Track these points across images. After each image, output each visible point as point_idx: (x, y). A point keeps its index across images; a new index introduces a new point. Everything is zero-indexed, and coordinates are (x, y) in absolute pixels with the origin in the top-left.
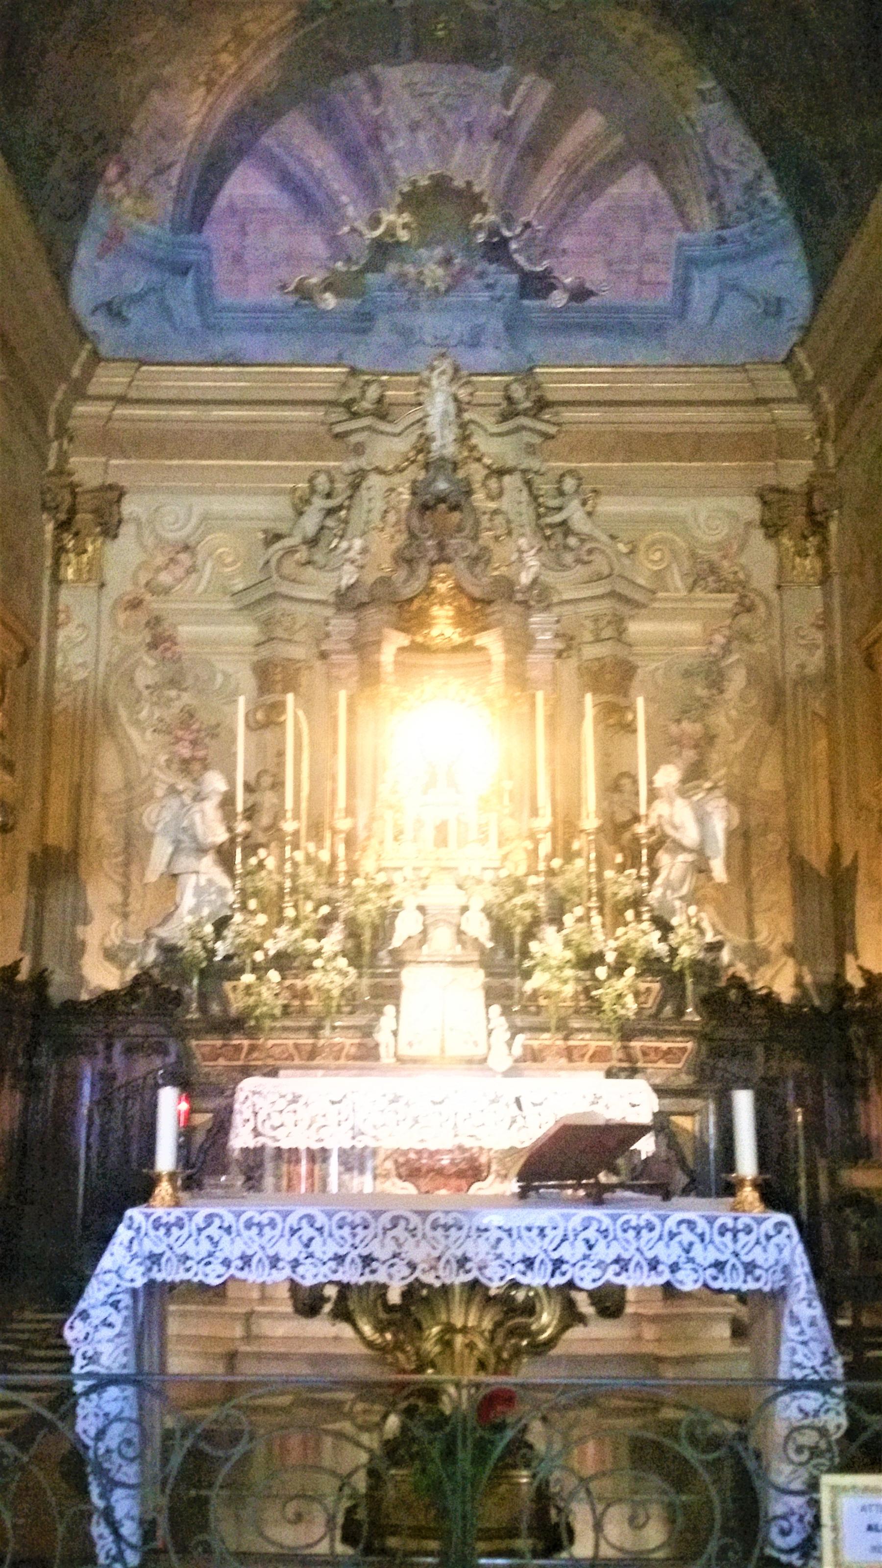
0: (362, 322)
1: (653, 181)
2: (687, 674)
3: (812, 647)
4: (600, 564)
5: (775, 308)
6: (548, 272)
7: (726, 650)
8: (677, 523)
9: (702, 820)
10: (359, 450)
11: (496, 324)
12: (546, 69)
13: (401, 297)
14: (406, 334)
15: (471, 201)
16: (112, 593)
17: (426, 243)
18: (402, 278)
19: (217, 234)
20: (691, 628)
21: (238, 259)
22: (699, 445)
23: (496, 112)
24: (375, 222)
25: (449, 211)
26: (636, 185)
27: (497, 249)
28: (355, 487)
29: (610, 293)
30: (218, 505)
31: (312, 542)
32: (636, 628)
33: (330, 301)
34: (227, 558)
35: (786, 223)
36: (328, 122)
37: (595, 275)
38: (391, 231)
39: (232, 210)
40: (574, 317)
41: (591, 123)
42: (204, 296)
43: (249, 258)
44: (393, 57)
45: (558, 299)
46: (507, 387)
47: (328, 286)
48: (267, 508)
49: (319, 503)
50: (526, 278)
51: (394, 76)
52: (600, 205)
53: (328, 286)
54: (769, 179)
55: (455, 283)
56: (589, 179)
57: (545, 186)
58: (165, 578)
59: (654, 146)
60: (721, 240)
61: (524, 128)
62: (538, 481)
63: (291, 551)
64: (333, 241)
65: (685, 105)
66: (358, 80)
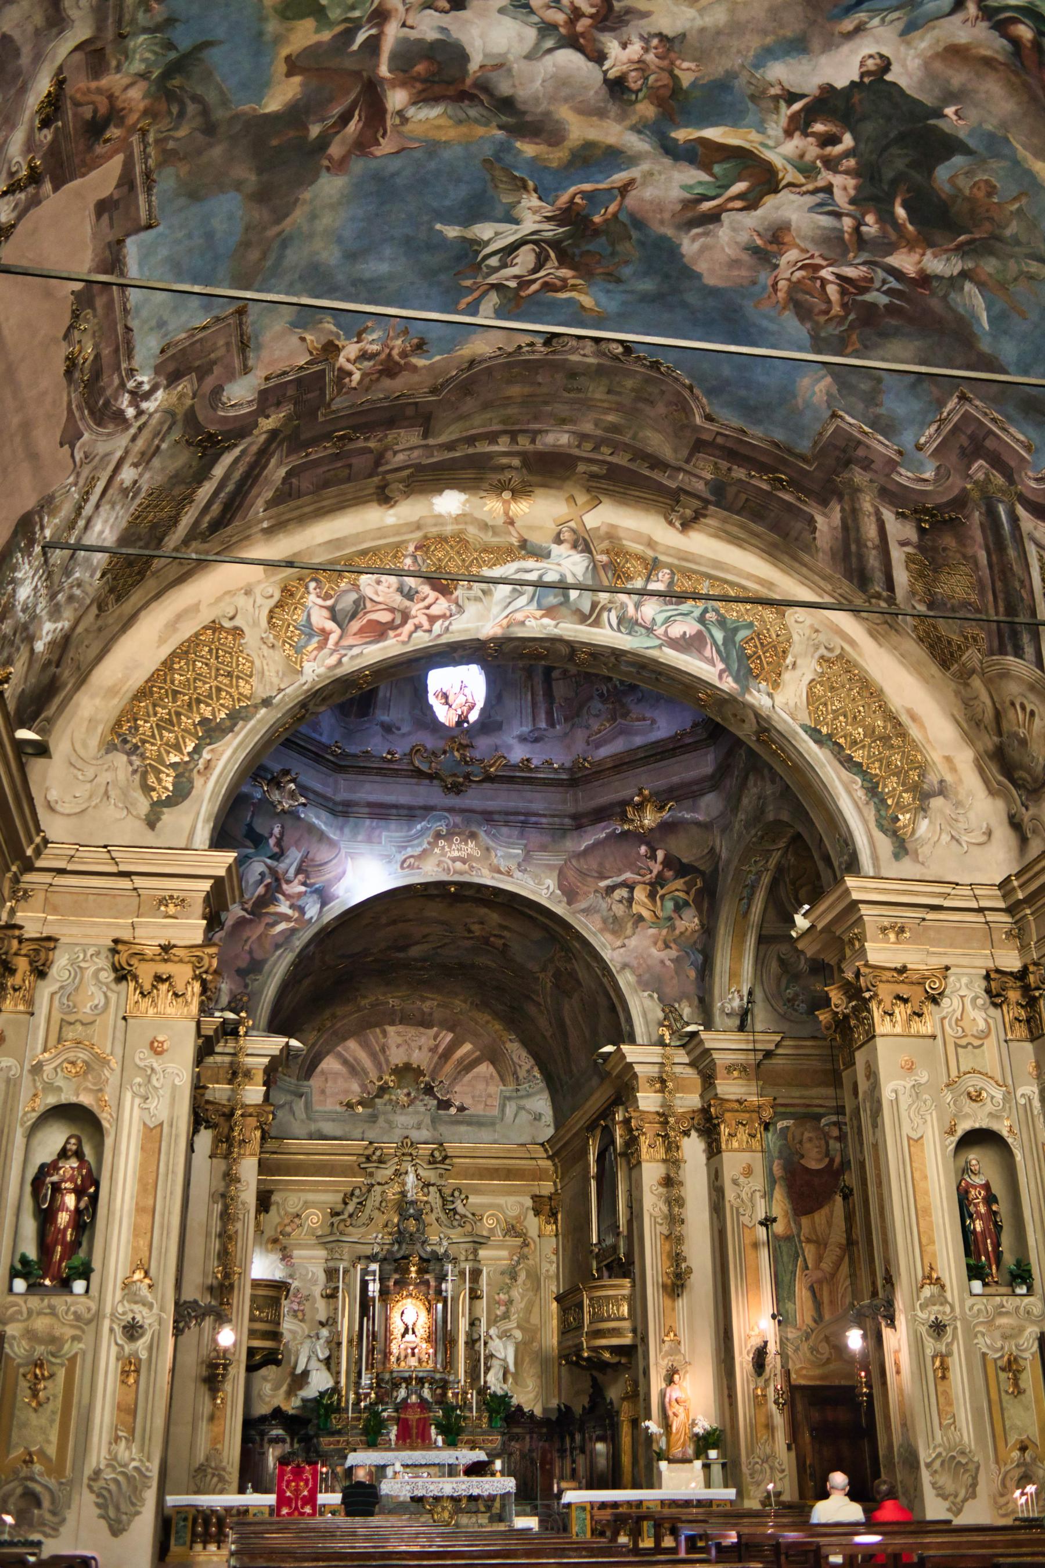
0: (373, 1118)
1: (491, 1068)
2: (502, 1273)
3: (551, 1262)
4: (468, 1228)
5: (538, 1117)
6: (449, 1100)
7: (518, 1263)
8: (499, 1207)
9: (505, 1348)
10: (371, 1175)
11: (428, 1120)
12: (451, 1029)
13: (389, 1108)
14: (389, 1122)
15: (419, 1072)
16: (266, 1236)
17: (399, 1087)
18: (391, 1100)
19: (315, 1082)
20: (504, 1253)
21: (323, 1092)
22: (509, 1174)
23: (432, 1043)
24: (380, 1078)
25: (410, 1077)
26: (485, 1069)
27: (429, 1090)
28: (369, 1191)
29: (475, 1110)
30: (311, 1197)
31: (351, 1216)
32: (482, 1253)
33: (360, 1109)
34: (315, 1219)
35: (542, 1085)
36: (365, 1045)
37: (468, 1102)
38: (386, 1083)
39: (323, 1072)
40: (460, 1118)
41: (467, 1047)
42: (308, 1106)
43: (328, 1091)
44: (392, 1023)
45: (453, 1111)
46: (434, 1150)
47: (360, 1103)
48: (334, 1199)
49: (355, 1200)
50: (440, 1102)
51: (391, 1030)
52: (470, 1075)
53: (360, 1103)
54: (536, 1069)
55: (411, 1103)
56: (467, 1066)
57: (449, 1067)
58: (288, 1229)
59: (494, 1056)
60: (518, 1090)
61: (440, 1050)
62: (444, 1190)
63: (344, 1220)
64: (363, 1087)
65: (504, 1043)
66: (378, 1030)
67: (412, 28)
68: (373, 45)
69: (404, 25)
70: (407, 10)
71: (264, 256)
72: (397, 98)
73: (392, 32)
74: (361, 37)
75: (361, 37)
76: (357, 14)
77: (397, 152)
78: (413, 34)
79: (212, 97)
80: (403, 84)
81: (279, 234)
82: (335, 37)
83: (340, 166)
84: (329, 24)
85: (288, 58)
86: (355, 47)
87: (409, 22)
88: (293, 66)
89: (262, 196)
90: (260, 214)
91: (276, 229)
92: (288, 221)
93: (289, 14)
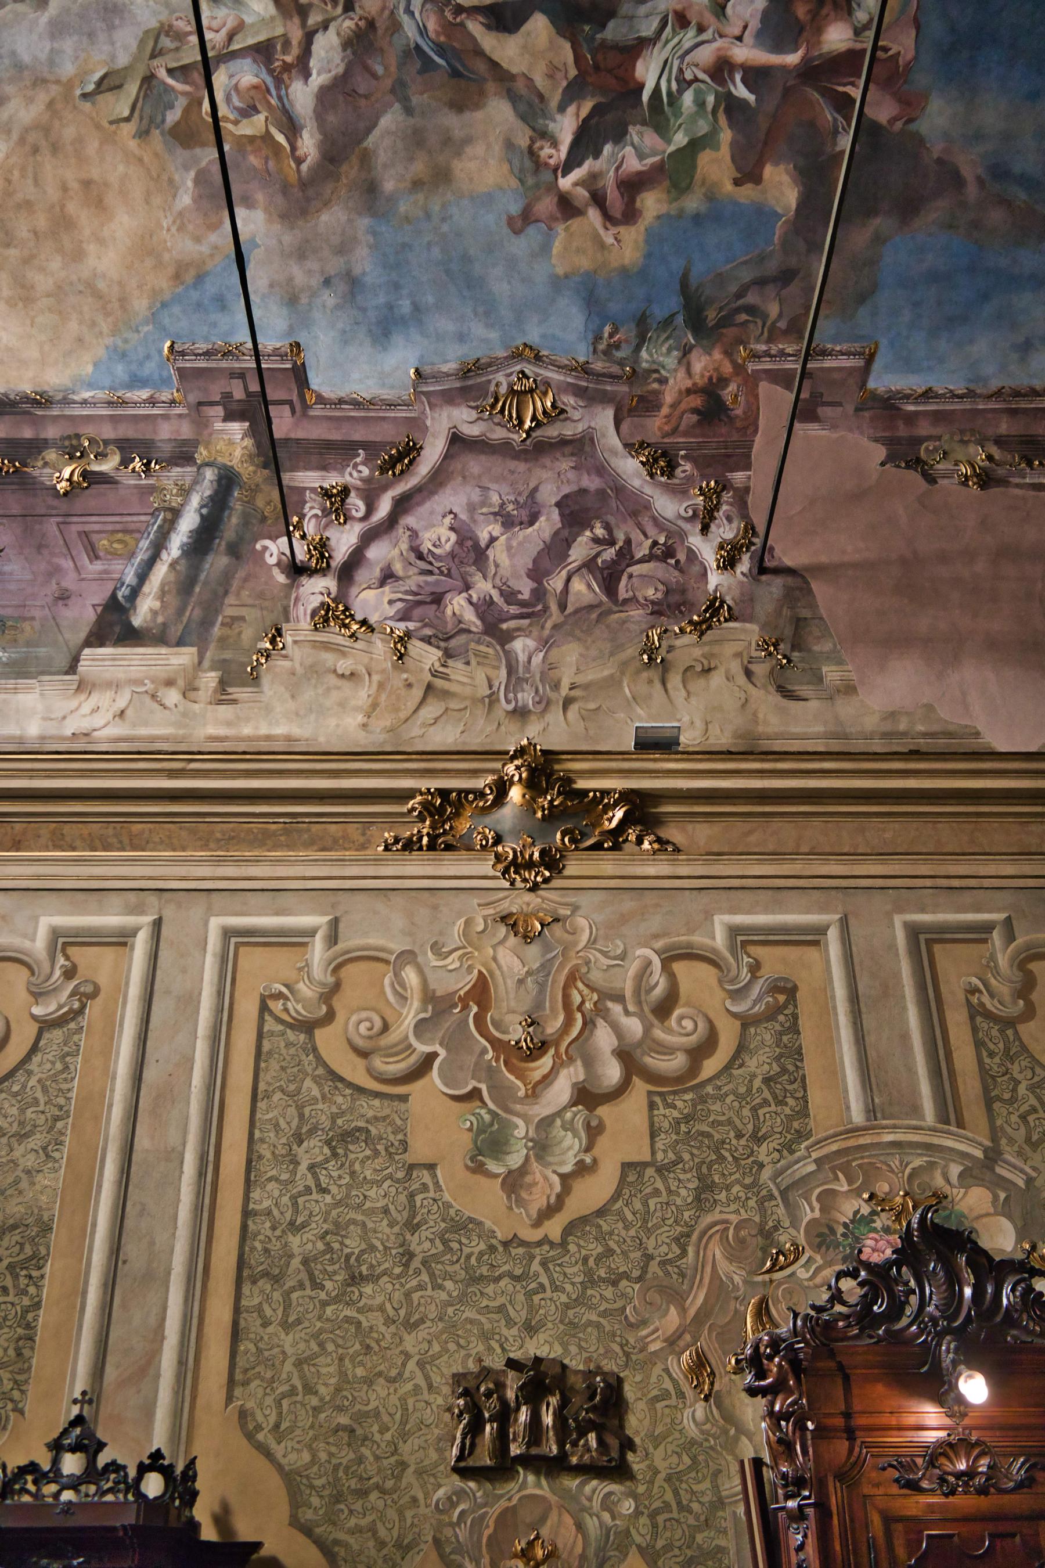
67: (745, 27)
68: (755, 76)
69: (740, 38)
70: (721, 36)
71: (1005, 202)
72: (837, 37)
73: (744, 53)
74: (741, 91)
75: (741, 91)
76: (711, 99)
77: (918, 29)
78: (755, 24)
79: (747, 275)
80: (819, 31)
81: (980, 181)
82: (730, 127)
83: (911, 105)
84: (714, 132)
85: (737, 182)
86: (751, 98)
87: (737, 31)
88: (749, 174)
89: (908, 209)
90: (936, 211)
91: (972, 191)
92: (968, 173)
93: (683, 185)
